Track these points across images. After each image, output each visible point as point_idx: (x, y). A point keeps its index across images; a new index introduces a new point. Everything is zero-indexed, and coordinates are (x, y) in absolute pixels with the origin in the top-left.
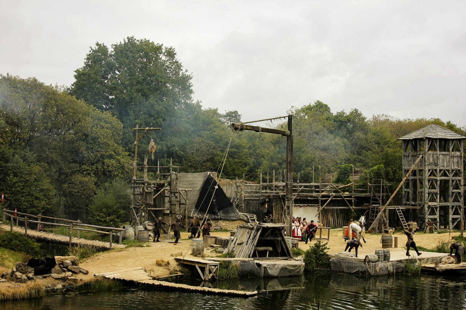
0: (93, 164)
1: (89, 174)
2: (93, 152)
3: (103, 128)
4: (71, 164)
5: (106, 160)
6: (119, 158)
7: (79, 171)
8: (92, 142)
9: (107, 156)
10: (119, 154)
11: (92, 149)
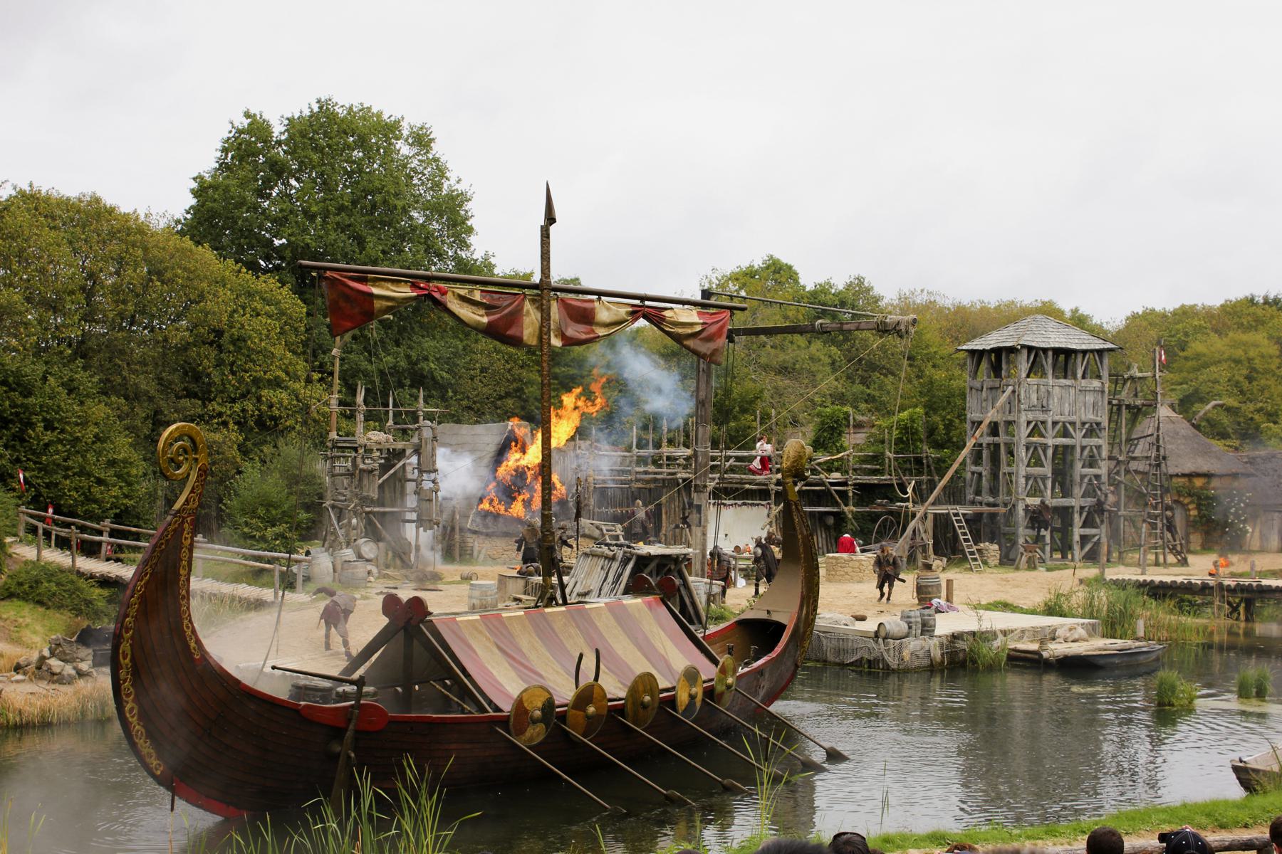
0: (233, 401)
1: (225, 424)
2: (233, 373)
3: (258, 315)
4: (183, 401)
5: (264, 392)
6: (297, 386)
7: (201, 417)
8: (232, 348)
9: (269, 381)
11: (232, 364)
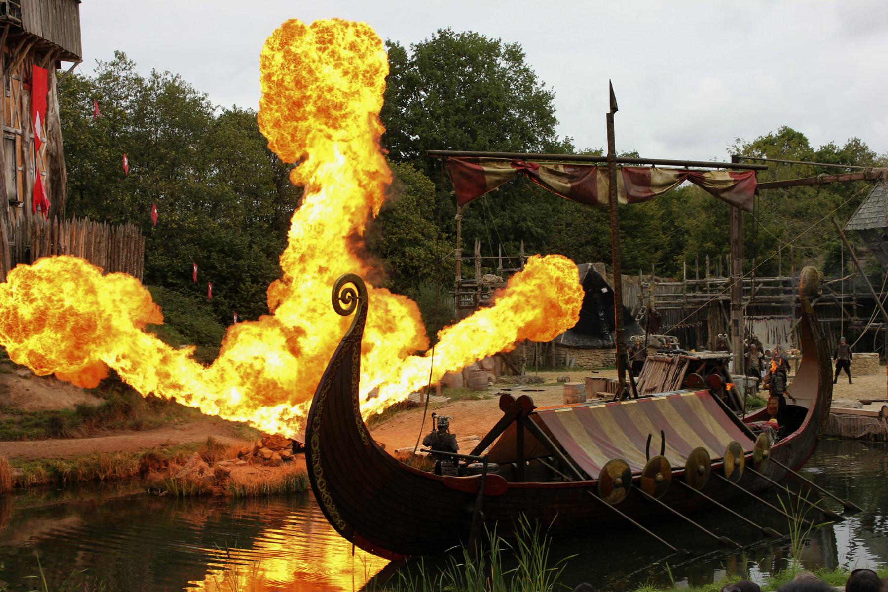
3: (400, 192)
5: (407, 249)
9: (410, 240)
10: (429, 238)
